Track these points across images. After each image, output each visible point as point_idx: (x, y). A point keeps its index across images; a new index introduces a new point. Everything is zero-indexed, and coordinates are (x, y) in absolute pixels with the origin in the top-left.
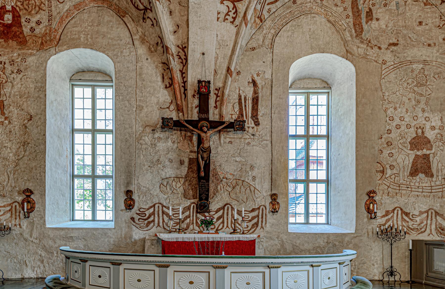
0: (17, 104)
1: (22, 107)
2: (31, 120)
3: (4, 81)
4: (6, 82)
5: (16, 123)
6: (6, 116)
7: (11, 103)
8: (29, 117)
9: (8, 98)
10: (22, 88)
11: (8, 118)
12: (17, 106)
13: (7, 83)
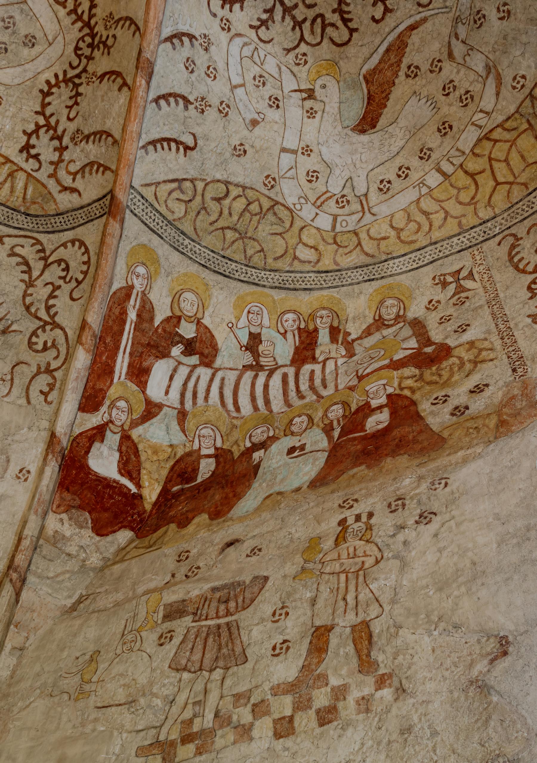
0: (427, 616)
1: (456, 619)
2: (505, 653)
3: (369, 562)
4: (377, 562)
5: (430, 686)
6: (382, 671)
7: (400, 619)
8: (492, 645)
9: (387, 608)
10: (443, 561)
11: (390, 676)
12: (429, 622)
13: (382, 564)
